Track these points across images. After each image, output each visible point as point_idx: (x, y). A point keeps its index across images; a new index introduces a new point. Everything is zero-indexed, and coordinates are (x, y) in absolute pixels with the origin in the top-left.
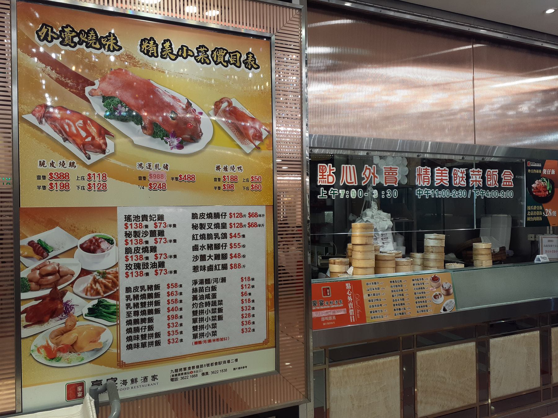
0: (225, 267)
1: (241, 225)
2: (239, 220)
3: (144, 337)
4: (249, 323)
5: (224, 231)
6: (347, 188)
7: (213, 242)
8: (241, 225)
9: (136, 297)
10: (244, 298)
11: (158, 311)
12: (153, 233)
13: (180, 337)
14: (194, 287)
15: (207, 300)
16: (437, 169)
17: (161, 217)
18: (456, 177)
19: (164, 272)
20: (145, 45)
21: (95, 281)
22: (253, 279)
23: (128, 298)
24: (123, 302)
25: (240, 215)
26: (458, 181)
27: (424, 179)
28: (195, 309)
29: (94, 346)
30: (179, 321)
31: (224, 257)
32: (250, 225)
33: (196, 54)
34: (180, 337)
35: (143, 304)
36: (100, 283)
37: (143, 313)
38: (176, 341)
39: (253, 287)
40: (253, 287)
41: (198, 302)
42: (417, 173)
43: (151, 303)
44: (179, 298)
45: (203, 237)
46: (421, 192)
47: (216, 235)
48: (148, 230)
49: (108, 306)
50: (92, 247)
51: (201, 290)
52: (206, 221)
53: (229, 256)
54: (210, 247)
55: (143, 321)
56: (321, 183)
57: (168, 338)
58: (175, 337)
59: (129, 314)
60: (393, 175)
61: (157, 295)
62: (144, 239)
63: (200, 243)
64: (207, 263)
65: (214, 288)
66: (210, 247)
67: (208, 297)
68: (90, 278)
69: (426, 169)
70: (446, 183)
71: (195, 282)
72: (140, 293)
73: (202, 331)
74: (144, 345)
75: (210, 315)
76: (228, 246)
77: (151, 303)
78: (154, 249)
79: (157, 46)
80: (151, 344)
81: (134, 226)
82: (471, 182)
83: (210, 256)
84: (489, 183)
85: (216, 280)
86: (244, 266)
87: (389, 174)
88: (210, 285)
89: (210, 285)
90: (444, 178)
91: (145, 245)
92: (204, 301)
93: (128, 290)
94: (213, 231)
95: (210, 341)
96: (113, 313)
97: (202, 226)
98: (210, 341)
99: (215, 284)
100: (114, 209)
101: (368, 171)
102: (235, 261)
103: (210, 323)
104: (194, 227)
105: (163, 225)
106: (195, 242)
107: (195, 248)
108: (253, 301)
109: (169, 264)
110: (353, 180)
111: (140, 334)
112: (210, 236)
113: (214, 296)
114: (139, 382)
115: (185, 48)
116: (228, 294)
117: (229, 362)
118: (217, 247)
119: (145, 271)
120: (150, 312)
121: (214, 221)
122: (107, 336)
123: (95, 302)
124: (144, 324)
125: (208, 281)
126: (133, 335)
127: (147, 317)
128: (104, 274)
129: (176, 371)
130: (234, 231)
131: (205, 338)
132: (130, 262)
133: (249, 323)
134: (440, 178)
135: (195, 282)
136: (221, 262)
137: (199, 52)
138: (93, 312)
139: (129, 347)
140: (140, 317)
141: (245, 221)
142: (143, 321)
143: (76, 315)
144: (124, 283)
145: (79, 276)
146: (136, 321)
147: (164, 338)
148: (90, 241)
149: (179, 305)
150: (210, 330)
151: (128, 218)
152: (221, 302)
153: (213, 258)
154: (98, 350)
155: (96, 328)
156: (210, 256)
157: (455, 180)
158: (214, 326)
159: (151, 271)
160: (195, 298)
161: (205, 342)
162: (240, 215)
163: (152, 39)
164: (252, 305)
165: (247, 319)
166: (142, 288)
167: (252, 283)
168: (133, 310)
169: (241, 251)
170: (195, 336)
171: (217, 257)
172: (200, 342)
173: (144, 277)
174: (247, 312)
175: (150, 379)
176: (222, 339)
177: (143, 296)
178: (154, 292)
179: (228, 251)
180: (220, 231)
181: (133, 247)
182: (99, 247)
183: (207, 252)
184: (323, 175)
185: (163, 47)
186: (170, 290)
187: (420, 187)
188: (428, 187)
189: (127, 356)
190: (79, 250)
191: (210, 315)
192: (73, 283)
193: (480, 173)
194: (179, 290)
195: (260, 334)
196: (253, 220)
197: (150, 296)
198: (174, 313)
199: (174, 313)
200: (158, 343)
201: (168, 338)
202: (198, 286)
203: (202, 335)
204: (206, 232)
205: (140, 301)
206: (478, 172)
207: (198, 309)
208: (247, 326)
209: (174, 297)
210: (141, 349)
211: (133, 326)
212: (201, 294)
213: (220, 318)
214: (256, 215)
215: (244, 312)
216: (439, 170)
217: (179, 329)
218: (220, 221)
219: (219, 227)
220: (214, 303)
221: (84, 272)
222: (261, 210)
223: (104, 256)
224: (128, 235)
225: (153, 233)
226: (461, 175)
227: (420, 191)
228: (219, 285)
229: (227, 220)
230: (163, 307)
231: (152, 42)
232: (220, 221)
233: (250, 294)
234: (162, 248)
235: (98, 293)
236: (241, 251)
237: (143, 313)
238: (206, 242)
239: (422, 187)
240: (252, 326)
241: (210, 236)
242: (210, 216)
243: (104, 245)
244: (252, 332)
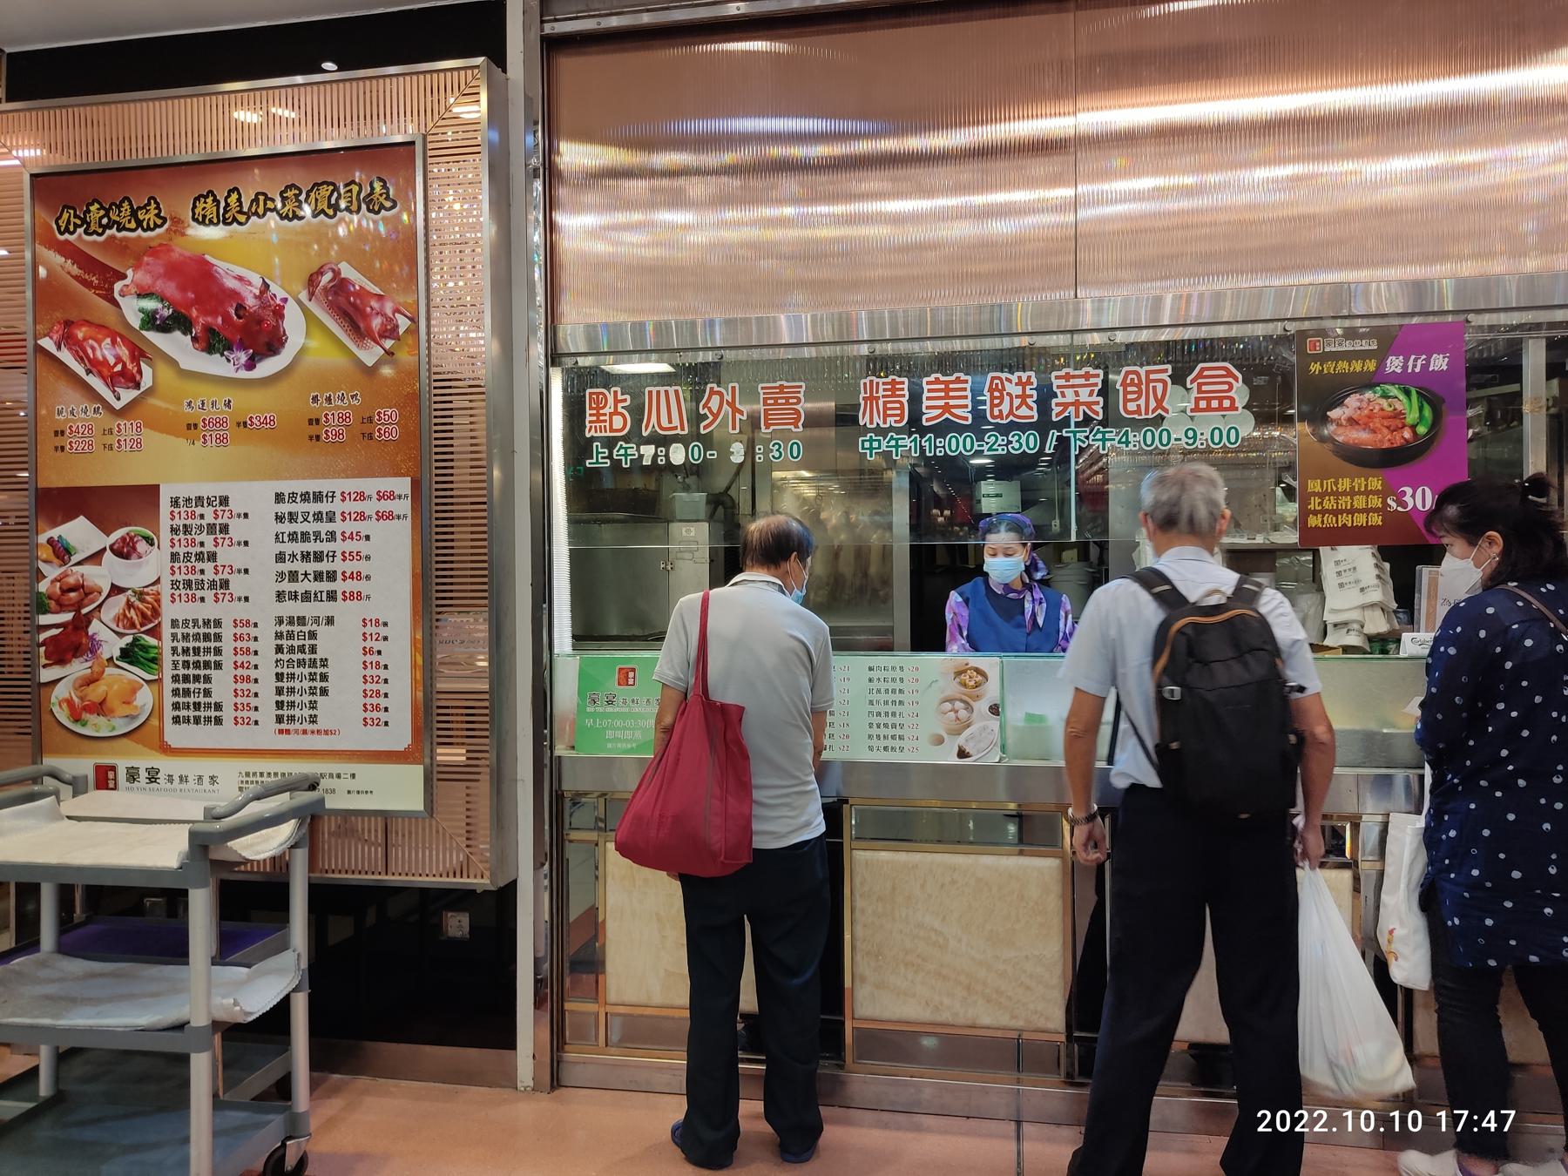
0: (332, 596)
1: (362, 516)
2: (358, 506)
3: (197, 706)
4: (377, 708)
5: (331, 527)
6: (662, 441)
7: (311, 547)
8: (362, 516)
9: (185, 637)
10: (368, 658)
11: (218, 665)
12: (211, 529)
13: (254, 715)
14: (279, 629)
15: (301, 656)
16: (932, 378)
17: (224, 501)
18: (1001, 398)
19: (228, 597)
20: (200, 205)
21: (129, 605)
22: (385, 624)
23: (174, 636)
24: (167, 643)
25: (361, 496)
26: (1005, 408)
27: (885, 409)
28: (279, 670)
29: (127, 710)
30: (254, 688)
31: (332, 576)
32: (381, 516)
33: (279, 206)
34: (254, 715)
35: (197, 651)
36: (137, 609)
37: (197, 665)
38: (247, 722)
39: (386, 639)
40: (386, 639)
41: (285, 657)
42: (862, 395)
43: (207, 650)
44: (253, 646)
45: (293, 537)
46: (875, 444)
47: (317, 535)
48: (204, 523)
49: (145, 648)
50: (124, 550)
51: (290, 635)
52: (299, 507)
53: (339, 576)
54: (306, 556)
55: (197, 678)
56: (593, 433)
57: (234, 714)
58: (245, 714)
59: (175, 664)
60: (787, 403)
61: (218, 637)
62: (198, 539)
63: (289, 548)
64: (300, 587)
65: (313, 635)
66: (306, 556)
67: (302, 649)
68: (121, 600)
69: (894, 382)
70: (964, 415)
71: (280, 621)
72: (191, 631)
73: (291, 712)
74: (197, 721)
75: (306, 684)
76: (339, 556)
77: (207, 650)
78: (212, 557)
79: (218, 203)
80: (208, 720)
81: (183, 515)
82: (1056, 410)
83: (306, 574)
84: (1132, 406)
85: (317, 620)
86: (368, 597)
87: (776, 403)
88: (305, 629)
89: (305, 629)
90: (952, 402)
91: (198, 549)
92: (295, 657)
93: (174, 623)
94: (311, 527)
95: (305, 732)
96: (154, 660)
97: (292, 517)
98: (305, 732)
99: (315, 627)
100: (155, 489)
101: (716, 398)
102: (351, 586)
103: (307, 698)
104: (279, 518)
105: (227, 514)
106: (280, 547)
107: (280, 558)
108: (386, 667)
109: (238, 585)
110: (676, 422)
111: (191, 700)
112: (305, 537)
113: (313, 649)
114: (192, 784)
115: (262, 198)
116: (340, 646)
117: (339, 776)
118: (319, 557)
119: (199, 594)
120: (207, 665)
121: (313, 507)
122: (145, 697)
123: (129, 639)
124: (197, 685)
125: (302, 621)
126: (181, 700)
127: (202, 672)
128: (140, 595)
129: (247, 774)
130: (350, 527)
131: (297, 725)
132: (177, 577)
133: (377, 708)
134: (942, 403)
135: (280, 621)
136: (325, 586)
137: (284, 199)
138: (126, 654)
139: (176, 720)
140: (191, 672)
141: (370, 507)
142: (197, 678)
143: (106, 656)
144: (169, 611)
145: (109, 596)
146: (186, 679)
147: (228, 714)
148: (123, 539)
149: (253, 659)
150: (307, 712)
151: (175, 502)
152: (324, 663)
153: (311, 577)
154: (133, 718)
155: (130, 681)
156: (306, 574)
157: (993, 406)
158: (313, 705)
159: (209, 595)
160: (279, 649)
161: (296, 731)
162: (361, 496)
163: (210, 192)
164: (383, 674)
165: (375, 701)
166: (195, 622)
167: (383, 631)
168: (181, 658)
169: (362, 566)
170: (279, 719)
171: (318, 576)
172: (288, 732)
173: (198, 603)
174: (375, 687)
175: (206, 780)
176: (326, 732)
177: (197, 637)
178: (212, 631)
179: (338, 566)
180: (324, 527)
181: (182, 550)
182: (134, 549)
183: (300, 566)
184: (598, 415)
185: (227, 205)
186: (239, 631)
187: (872, 430)
188: (898, 431)
189: (175, 735)
190: (108, 553)
191: (306, 684)
192: (100, 606)
193: (1092, 380)
194: (253, 632)
195: (400, 735)
196: (386, 506)
197: (207, 637)
198: (245, 672)
199: (245, 672)
200: (218, 721)
201: (234, 714)
202: (284, 628)
203: (292, 719)
204: (299, 527)
205: (191, 645)
206: (1087, 376)
207: (285, 671)
208: (374, 713)
209: (244, 644)
210: (192, 726)
211: (181, 686)
212: (290, 643)
213: (324, 692)
214: (390, 496)
215: (368, 687)
216: (937, 381)
217: (254, 702)
218: (324, 507)
219: (321, 520)
220: (313, 663)
221: (116, 590)
222: (403, 485)
223: (140, 565)
224: (174, 530)
225: (211, 529)
226: (1018, 390)
227: (871, 440)
228: (322, 630)
229: (337, 506)
230: (227, 659)
231: (210, 200)
232: (324, 507)
233: (379, 652)
234: (226, 555)
235: (133, 626)
236: (362, 566)
237: (197, 665)
238: (299, 548)
239: (880, 431)
240: (383, 716)
241: (305, 537)
242: (305, 497)
243: (142, 546)
244: (383, 728)
